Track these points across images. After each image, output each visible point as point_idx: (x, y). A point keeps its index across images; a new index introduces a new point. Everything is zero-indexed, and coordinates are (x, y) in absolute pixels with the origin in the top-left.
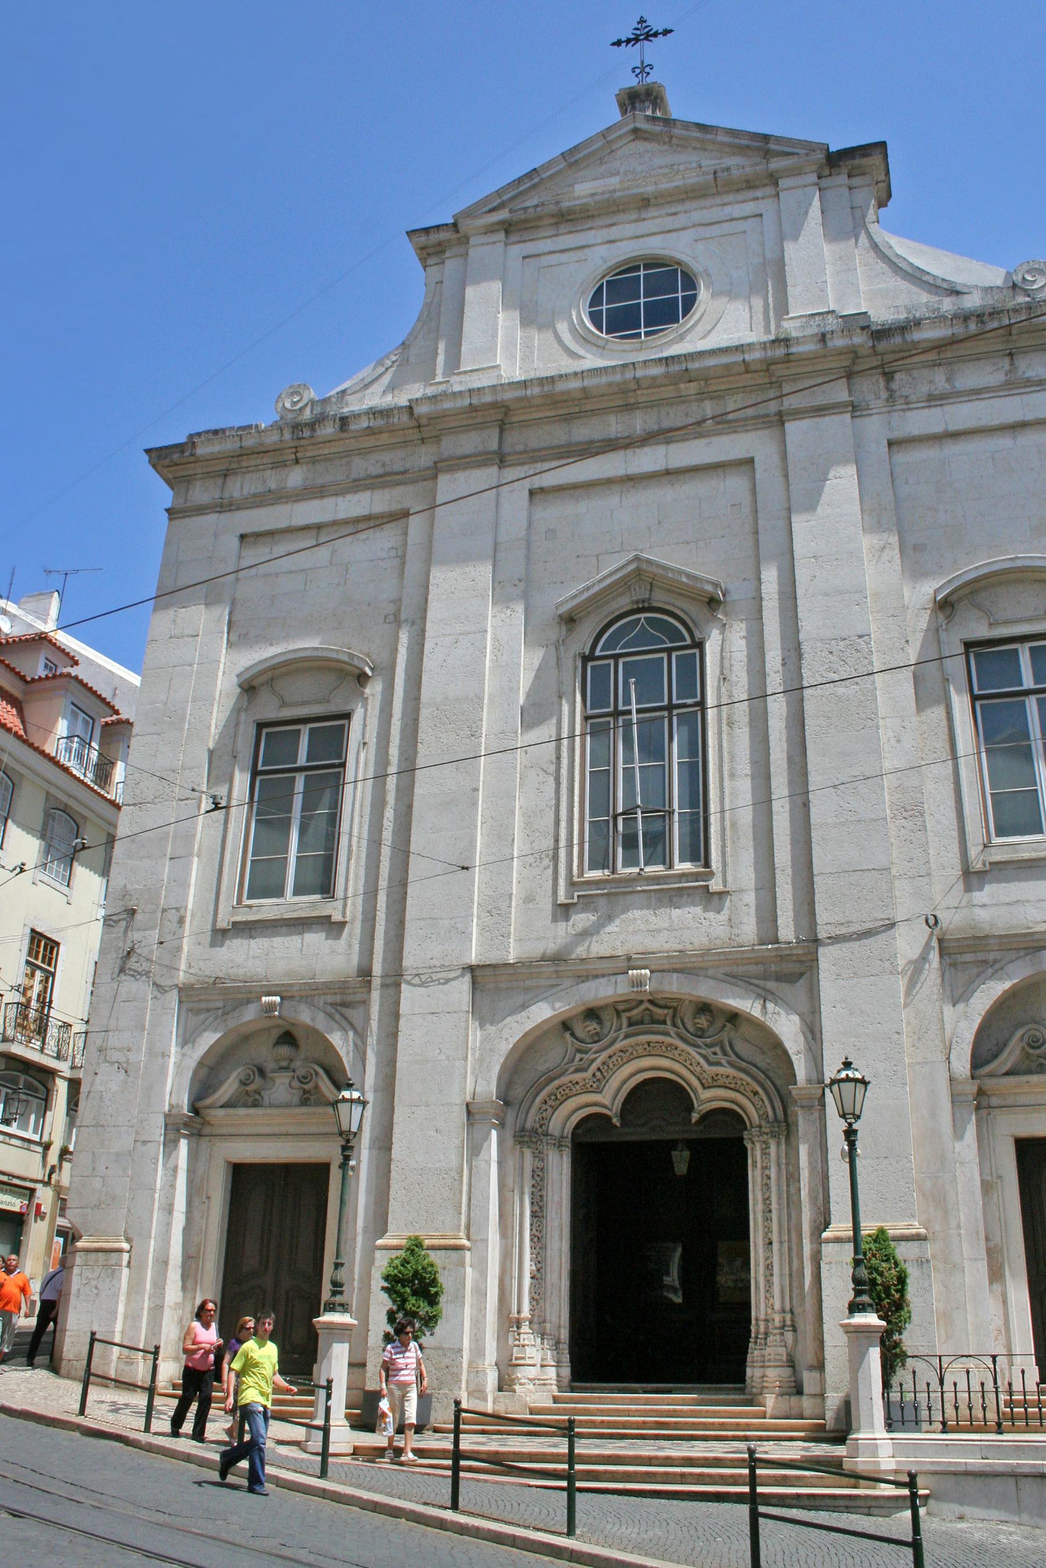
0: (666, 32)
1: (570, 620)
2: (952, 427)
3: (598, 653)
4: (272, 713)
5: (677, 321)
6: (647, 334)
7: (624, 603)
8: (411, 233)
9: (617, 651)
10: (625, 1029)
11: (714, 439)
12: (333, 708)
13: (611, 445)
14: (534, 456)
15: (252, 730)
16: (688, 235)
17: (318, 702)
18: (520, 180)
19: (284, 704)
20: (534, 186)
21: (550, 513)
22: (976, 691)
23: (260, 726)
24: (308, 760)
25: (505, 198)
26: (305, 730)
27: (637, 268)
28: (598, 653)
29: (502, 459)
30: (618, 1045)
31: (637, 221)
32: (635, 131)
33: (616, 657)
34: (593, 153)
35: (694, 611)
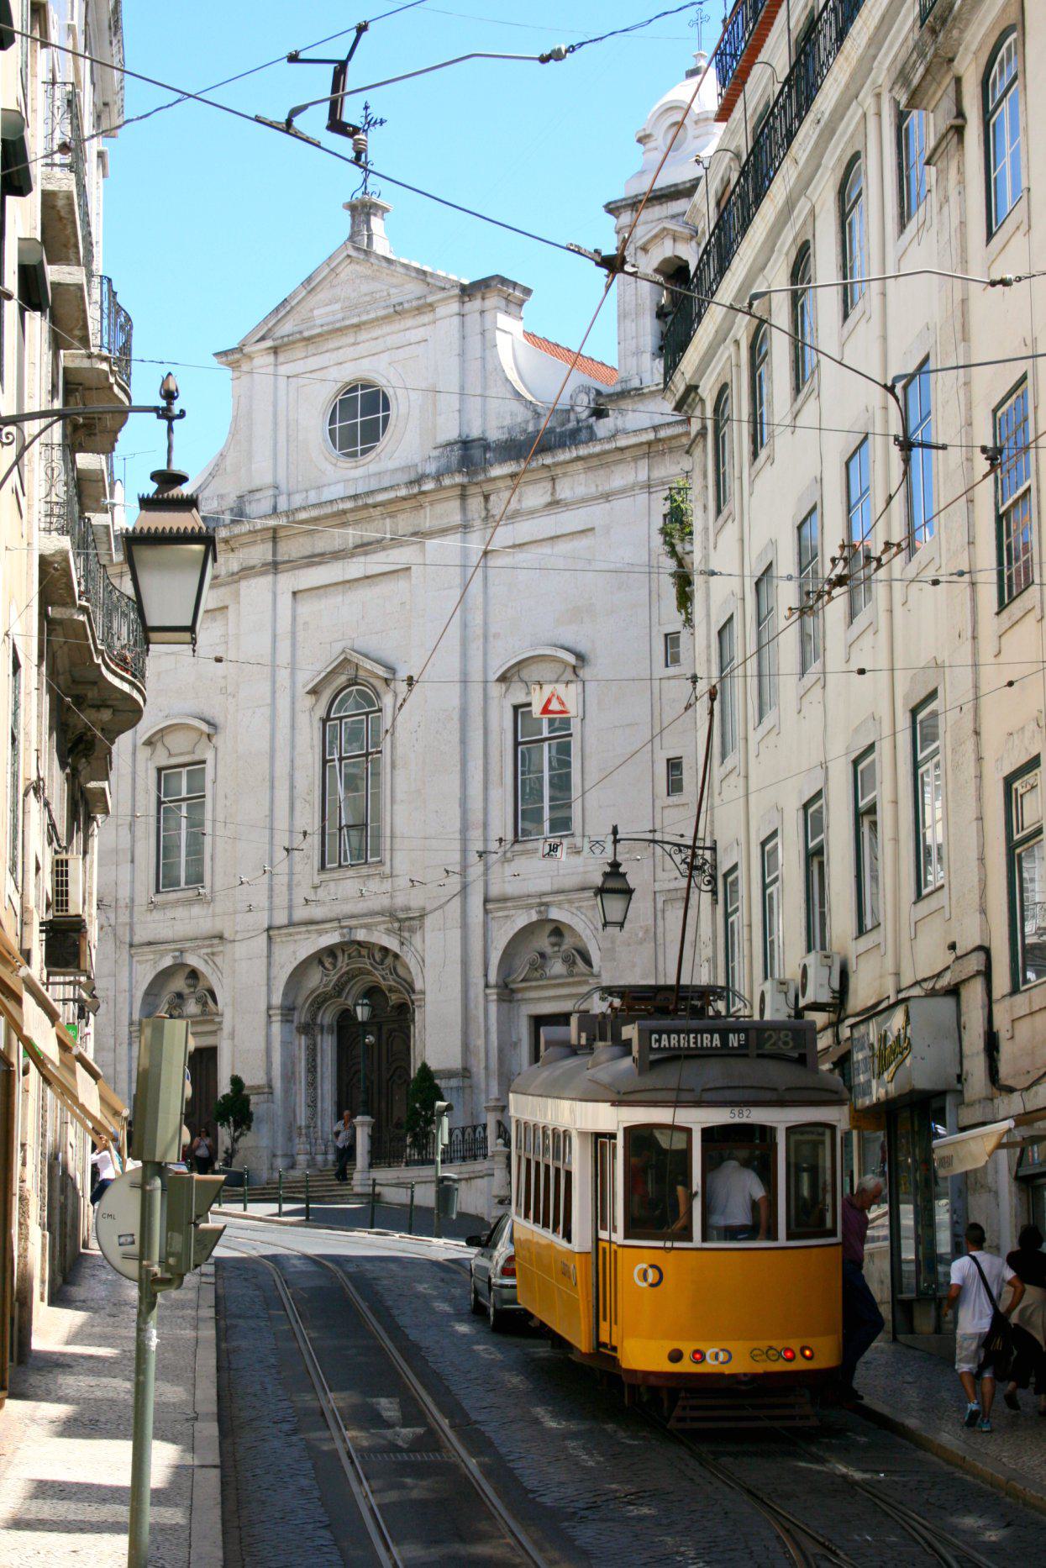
0: (382, 122)
1: (314, 692)
2: (517, 542)
3: (332, 716)
4: (165, 762)
5: (378, 440)
6: (364, 452)
7: (342, 679)
8: (216, 355)
9: (342, 714)
10: (346, 961)
11: (390, 552)
12: (196, 758)
13: (337, 555)
14: (296, 564)
15: (153, 774)
16: (385, 357)
17: (188, 753)
18: (277, 310)
19: (170, 755)
20: (288, 312)
21: (306, 608)
22: (520, 740)
23: (159, 770)
24: (188, 793)
25: (270, 325)
26: (184, 771)
27: (354, 389)
28: (332, 716)
29: (274, 567)
30: (343, 971)
31: (354, 344)
32: (349, 256)
33: (341, 719)
34: (324, 279)
35: (379, 685)
